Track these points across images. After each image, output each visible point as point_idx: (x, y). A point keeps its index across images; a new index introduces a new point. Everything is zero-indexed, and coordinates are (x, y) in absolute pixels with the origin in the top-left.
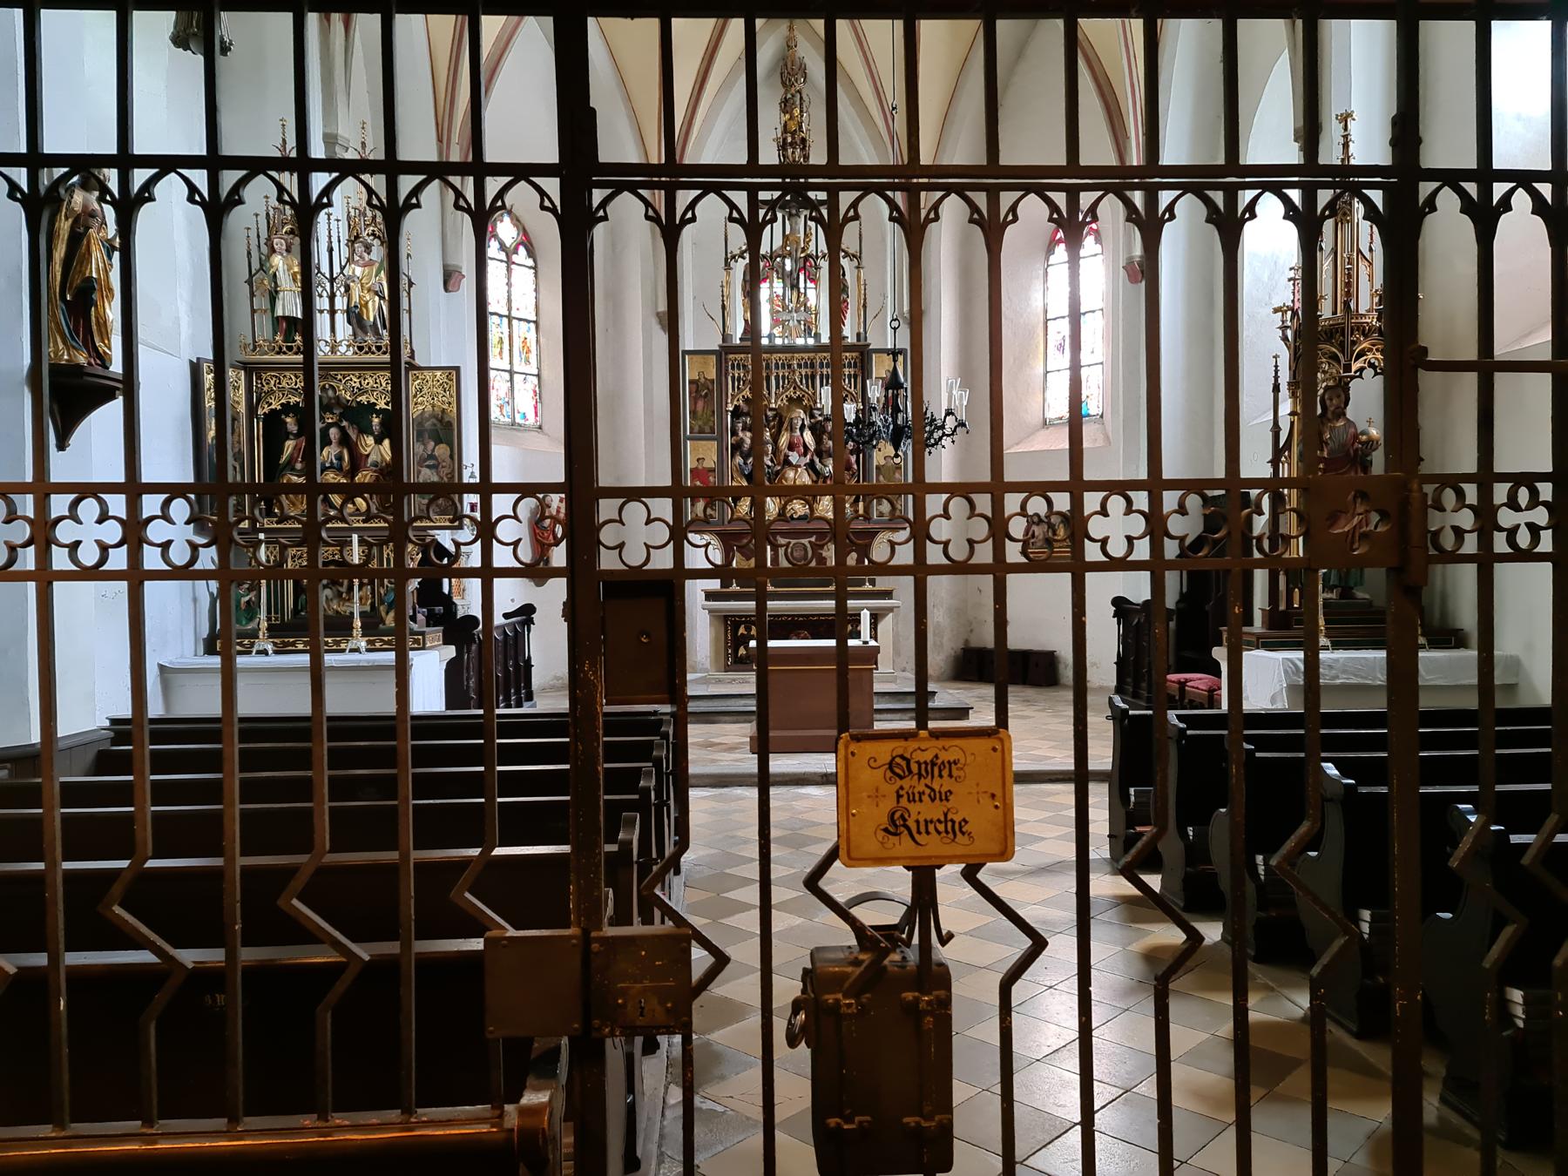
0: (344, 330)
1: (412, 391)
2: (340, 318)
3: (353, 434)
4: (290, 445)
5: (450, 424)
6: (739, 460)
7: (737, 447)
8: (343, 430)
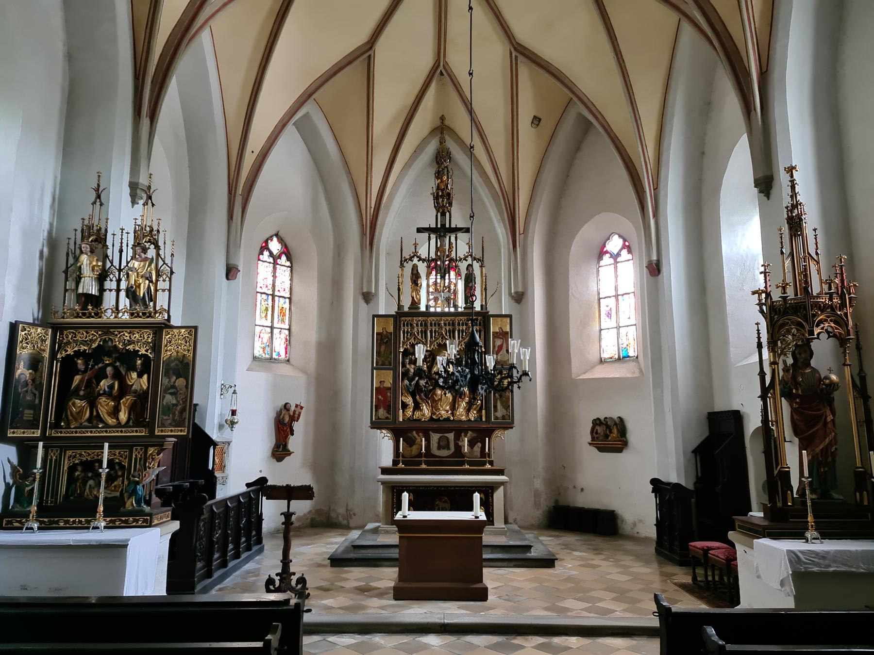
2: (123, 294)
6: (406, 382)
7: (405, 374)
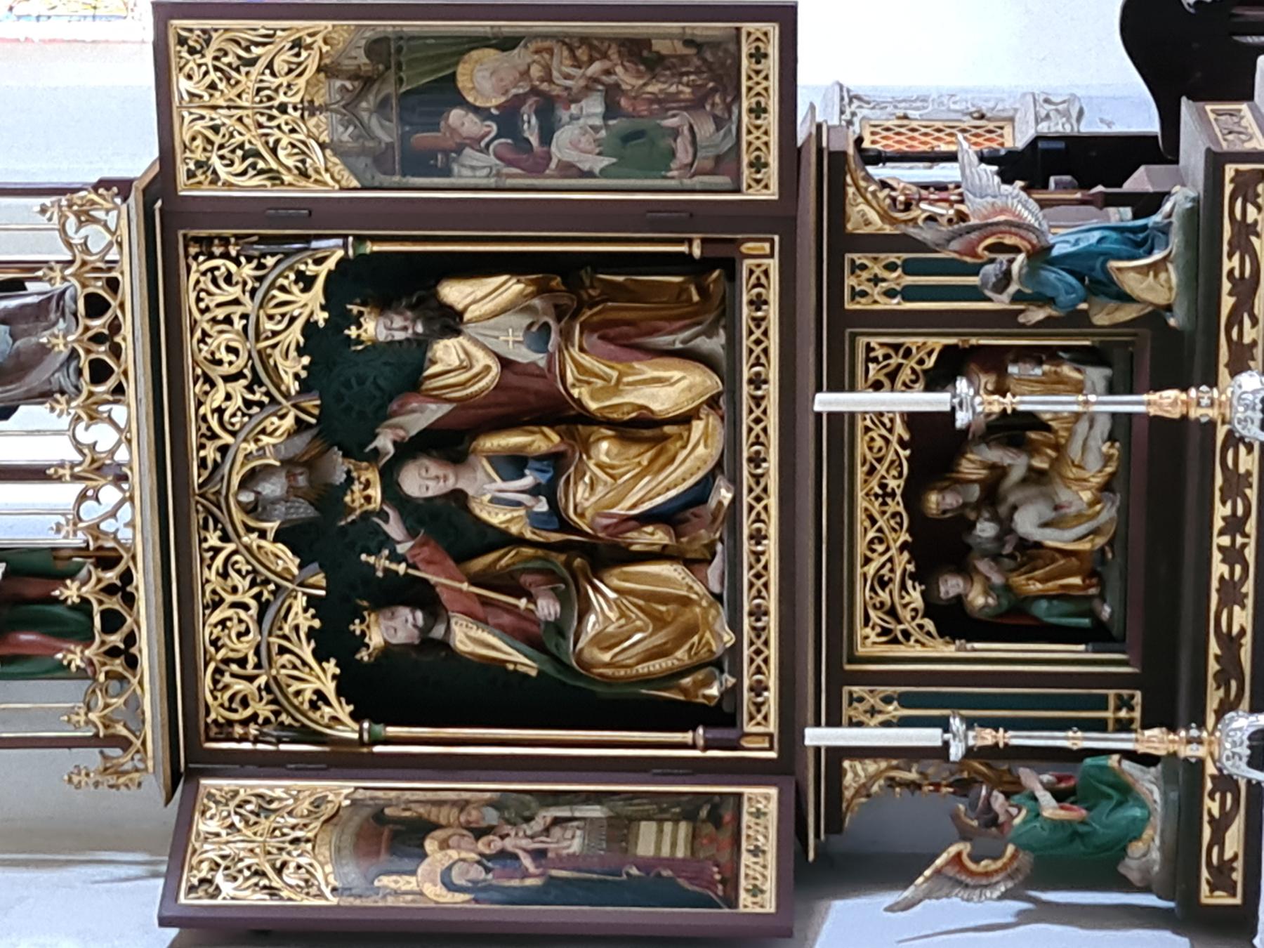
1: (252, 186)
3: (421, 416)
4: (468, 637)
5: (376, 48)
8: (409, 450)
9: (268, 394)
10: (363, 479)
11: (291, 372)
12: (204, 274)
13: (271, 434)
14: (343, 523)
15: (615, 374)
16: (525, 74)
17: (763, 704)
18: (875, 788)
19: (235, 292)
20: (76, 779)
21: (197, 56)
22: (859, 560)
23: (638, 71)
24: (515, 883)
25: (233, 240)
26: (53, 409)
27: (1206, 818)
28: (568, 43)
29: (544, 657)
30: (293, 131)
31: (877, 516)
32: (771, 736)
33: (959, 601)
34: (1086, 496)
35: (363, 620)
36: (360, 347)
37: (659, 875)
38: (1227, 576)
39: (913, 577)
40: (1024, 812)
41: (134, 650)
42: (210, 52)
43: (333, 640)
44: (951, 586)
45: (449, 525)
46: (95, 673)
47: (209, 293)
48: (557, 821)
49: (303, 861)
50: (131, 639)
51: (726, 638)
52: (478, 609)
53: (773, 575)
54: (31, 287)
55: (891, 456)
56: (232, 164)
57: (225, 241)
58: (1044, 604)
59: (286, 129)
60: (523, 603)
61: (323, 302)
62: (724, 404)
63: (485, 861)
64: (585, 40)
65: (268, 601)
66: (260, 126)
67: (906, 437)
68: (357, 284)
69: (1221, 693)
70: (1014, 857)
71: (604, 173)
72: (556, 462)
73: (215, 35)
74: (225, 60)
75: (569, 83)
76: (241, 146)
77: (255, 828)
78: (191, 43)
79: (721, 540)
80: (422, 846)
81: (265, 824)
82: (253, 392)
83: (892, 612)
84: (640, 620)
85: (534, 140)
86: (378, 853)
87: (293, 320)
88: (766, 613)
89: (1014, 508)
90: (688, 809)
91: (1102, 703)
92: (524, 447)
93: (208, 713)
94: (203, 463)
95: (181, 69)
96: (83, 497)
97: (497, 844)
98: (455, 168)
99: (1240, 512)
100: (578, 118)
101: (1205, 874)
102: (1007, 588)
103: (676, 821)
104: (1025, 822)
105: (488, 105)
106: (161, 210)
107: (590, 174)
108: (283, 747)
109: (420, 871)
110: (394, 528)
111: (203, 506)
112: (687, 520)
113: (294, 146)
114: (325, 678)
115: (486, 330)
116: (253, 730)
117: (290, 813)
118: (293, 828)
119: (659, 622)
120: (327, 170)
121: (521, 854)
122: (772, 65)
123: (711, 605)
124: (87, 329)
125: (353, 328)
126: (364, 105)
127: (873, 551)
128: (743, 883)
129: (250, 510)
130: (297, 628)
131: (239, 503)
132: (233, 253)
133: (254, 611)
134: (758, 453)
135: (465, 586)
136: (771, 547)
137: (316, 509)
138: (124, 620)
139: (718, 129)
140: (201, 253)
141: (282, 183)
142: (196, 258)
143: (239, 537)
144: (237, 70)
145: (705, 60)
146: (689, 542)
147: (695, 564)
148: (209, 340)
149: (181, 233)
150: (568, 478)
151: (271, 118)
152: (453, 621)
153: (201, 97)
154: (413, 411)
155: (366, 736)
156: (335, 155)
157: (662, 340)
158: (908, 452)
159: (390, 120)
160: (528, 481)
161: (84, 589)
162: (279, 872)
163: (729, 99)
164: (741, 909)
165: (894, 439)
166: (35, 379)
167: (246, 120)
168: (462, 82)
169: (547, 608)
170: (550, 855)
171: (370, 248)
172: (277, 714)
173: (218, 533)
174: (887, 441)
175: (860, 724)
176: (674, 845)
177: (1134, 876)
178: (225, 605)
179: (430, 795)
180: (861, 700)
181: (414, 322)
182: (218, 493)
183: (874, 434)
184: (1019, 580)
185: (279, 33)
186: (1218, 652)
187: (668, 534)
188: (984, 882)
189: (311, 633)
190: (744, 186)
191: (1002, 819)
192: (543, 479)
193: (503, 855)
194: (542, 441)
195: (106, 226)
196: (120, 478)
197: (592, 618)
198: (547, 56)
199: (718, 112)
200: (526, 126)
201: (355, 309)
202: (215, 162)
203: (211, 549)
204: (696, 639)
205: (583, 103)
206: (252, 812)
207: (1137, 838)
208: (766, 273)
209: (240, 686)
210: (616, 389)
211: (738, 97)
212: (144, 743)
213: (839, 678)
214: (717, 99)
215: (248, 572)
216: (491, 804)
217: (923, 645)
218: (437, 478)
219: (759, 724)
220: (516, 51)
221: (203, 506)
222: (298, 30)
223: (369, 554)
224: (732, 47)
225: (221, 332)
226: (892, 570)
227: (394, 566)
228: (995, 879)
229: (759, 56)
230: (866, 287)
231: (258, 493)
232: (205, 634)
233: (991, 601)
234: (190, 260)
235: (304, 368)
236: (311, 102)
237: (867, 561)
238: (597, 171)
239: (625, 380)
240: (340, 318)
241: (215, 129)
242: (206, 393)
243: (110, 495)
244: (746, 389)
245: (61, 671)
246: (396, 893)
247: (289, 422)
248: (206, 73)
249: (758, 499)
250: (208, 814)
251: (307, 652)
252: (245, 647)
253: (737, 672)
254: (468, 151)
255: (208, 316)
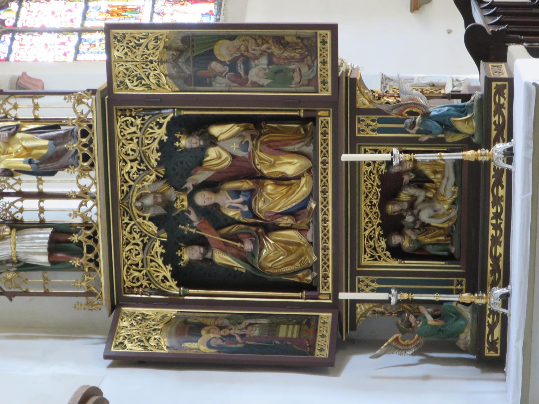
0: (64, 181)
1: (140, 91)
2: (50, 185)
5: (186, 40)
8: (198, 187)
9: (146, 166)
10: (181, 198)
11: (154, 158)
12: (123, 122)
13: (147, 181)
14: (174, 215)
15: (273, 160)
16: (239, 49)
17: (327, 282)
18: (368, 314)
19: (133, 129)
20: (77, 307)
21: (120, 43)
22: (362, 230)
23: (280, 48)
24: (233, 346)
25: (133, 110)
26: (68, 171)
27: (487, 324)
28: (253, 37)
29: (247, 265)
30: (155, 70)
31: (369, 213)
32: (330, 294)
33: (400, 246)
34: (446, 207)
35: (181, 250)
36: (180, 150)
37: (286, 344)
38: (494, 235)
39: (382, 236)
40: (421, 322)
41: (97, 260)
42: (125, 42)
43: (170, 258)
44: (396, 240)
45: (213, 216)
46: (84, 268)
47: (125, 130)
48: (250, 324)
49: (157, 337)
50: (97, 256)
51: (314, 258)
52: (223, 247)
53: (330, 235)
54: (62, 128)
55: (374, 191)
56: (133, 82)
57: (131, 110)
58: (431, 247)
59: (152, 69)
60: (239, 245)
61: (166, 132)
62: (312, 171)
63: (223, 338)
64: (260, 37)
65: (146, 243)
66: (143, 68)
67: (379, 184)
68: (179, 125)
69: (492, 278)
70: (418, 339)
71: (268, 86)
72: (252, 192)
73: (127, 35)
74: (130, 44)
75: (255, 52)
76: (136, 76)
77: (140, 325)
78: (119, 38)
79: (312, 222)
80: (200, 332)
81: (144, 324)
82: (141, 166)
83: (375, 249)
84: (281, 250)
85: (242, 73)
86: (184, 334)
87: (155, 139)
88: (328, 249)
89: (420, 211)
90: (298, 321)
91: (451, 283)
92: (240, 187)
93: (125, 284)
94: (123, 192)
95: (115, 48)
96: (81, 205)
97: (228, 332)
98: (214, 83)
99: (499, 211)
100: (258, 65)
101: (486, 345)
102: (417, 241)
103: (294, 325)
104: (422, 326)
105: (225, 60)
106: (108, 99)
107: (262, 86)
108: (152, 296)
109: (199, 341)
110: (193, 216)
111: (123, 207)
112: (300, 215)
113: (155, 75)
114: (166, 271)
115: (225, 144)
116: (141, 290)
117: (153, 320)
118: (154, 325)
119: (290, 253)
120: (167, 84)
121: (236, 335)
122: (329, 46)
123: (308, 246)
124: (81, 142)
125: (177, 143)
126: (180, 60)
127: (367, 226)
128: (317, 347)
129: (141, 209)
130: (157, 253)
131: (136, 207)
132: (133, 115)
133: (141, 246)
134: (325, 189)
135: (218, 238)
136: (330, 224)
137: (165, 210)
138: (94, 249)
139: (309, 69)
140: (122, 115)
141: (151, 89)
142: (120, 116)
143: (136, 219)
144: (135, 48)
145: (304, 44)
146: (301, 223)
147: (302, 231)
148: (124, 147)
149: (114, 107)
150: (256, 199)
151: (147, 65)
152: (214, 251)
153: (122, 58)
154: (200, 174)
155: (181, 293)
156: (170, 79)
157: (290, 148)
158: (380, 190)
159: (189, 66)
160: (241, 199)
161: (79, 237)
162: (148, 340)
163: (313, 58)
164: (316, 356)
165: (375, 184)
166: (63, 161)
167: (138, 66)
168: (216, 52)
169: (248, 246)
170: (247, 336)
171: (184, 113)
172: (150, 284)
173: (128, 218)
174: (372, 185)
175: (363, 291)
176: (292, 333)
177: (462, 346)
178: (131, 244)
179: (205, 315)
180: (363, 281)
181: (200, 140)
182: (128, 203)
183: (367, 183)
184: (422, 238)
185: (150, 34)
186: (492, 263)
187: (293, 220)
188: (407, 348)
189: (162, 255)
190: (319, 90)
191: (413, 325)
192: (246, 199)
193: (230, 336)
194: (246, 185)
195: (87, 105)
196: (93, 198)
197: (265, 251)
198: (247, 43)
199: (309, 63)
200: (239, 68)
201: (178, 136)
202: (127, 81)
203: (126, 223)
204: (303, 258)
205: (260, 60)
206: (139, 319)
207: (462, 332)
208: (327, 123)
209: (136, 274)
210: (273, 165)
211: (316, 58)
212: (101, 294)
213: (355, 273)
214: (309, 58)
215: (139, 232)
216: (227, 318)
217: (386, 261)
218: (208, 199)
219: (325, 290)
220: (235, 41)
221: (123, 207)
222: (157, 33)
223: (182, 225)
224: (314, 39)
225: (129, 144)
226: (374, 233)
227: (191, 230)
228: (410, 347)
229: (324, 42)
230: (364, 128)
231: (143, 203)
232: (123, 255)
233: (411, 245)
234: (118, 117)
235: (159, 157)
236: (161, 59)
237: (365, 230)
238: (265, 84)
239: (277, 162)
240: (172, 139)
241: (127, 69)
242: (124, 166)
243: (90, 203)
244: (320, 166)
245: (72, 268)
246: (190, 349)
247: (153, 177)
248: (124, 49)
249: (325, 206)
250: (123, 320)
251: (160, 261)
252: (138, 259)
253: (318, 271)
254: (218, 77)
255: (125, 138)
